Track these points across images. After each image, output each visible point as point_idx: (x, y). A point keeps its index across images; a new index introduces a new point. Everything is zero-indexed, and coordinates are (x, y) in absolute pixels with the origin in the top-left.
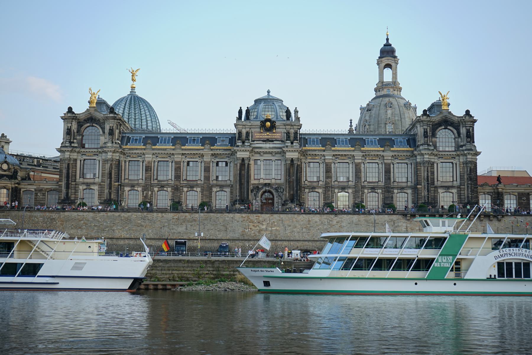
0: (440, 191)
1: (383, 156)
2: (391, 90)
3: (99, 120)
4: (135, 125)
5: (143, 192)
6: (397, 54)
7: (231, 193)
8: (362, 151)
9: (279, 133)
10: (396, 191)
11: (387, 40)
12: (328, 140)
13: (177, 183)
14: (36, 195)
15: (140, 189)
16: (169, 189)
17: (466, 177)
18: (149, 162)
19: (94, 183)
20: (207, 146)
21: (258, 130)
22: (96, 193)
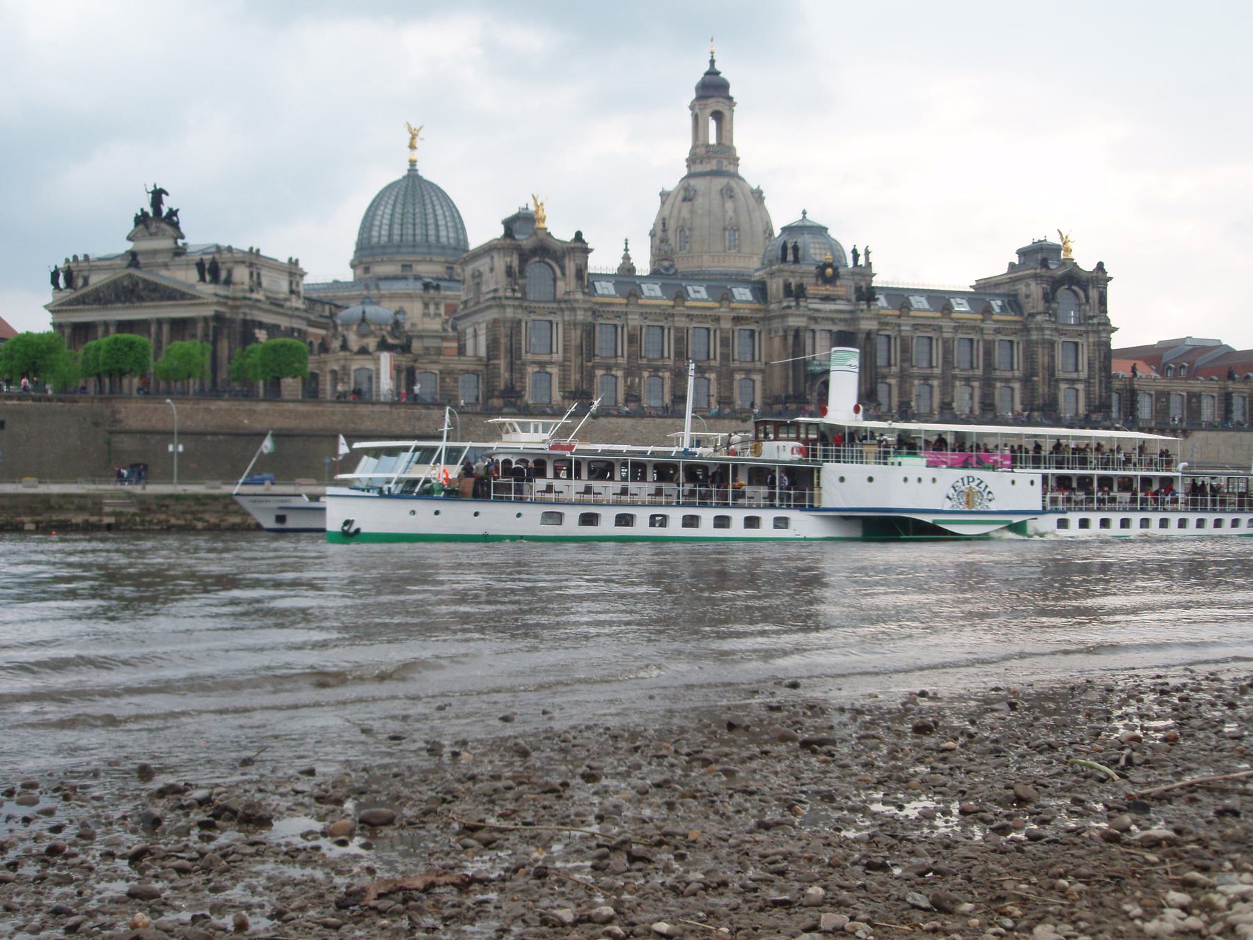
0: (1063, 386)
1: (982, 329)
2: (725, 163)
3: (555, 252)
4: (414, 235)
5: (625, 378)
6: (731, 93)
7: (764, 382)
8: (952, 319)
9: (844, 287)
10: (998, 385)
11: (712, 62)
12: (900, 297)
13: (679, 364)
14: (443, 380)
15: (620, 373)
16: (667, 375)
17: (1097, 365)
18: (634, 328)
19: (551, 363)
20: (725, 303)
21: (813, 280)
22: (555, 381)
